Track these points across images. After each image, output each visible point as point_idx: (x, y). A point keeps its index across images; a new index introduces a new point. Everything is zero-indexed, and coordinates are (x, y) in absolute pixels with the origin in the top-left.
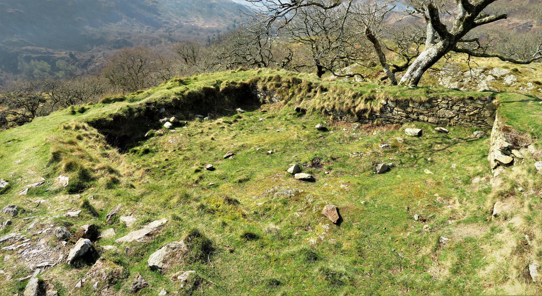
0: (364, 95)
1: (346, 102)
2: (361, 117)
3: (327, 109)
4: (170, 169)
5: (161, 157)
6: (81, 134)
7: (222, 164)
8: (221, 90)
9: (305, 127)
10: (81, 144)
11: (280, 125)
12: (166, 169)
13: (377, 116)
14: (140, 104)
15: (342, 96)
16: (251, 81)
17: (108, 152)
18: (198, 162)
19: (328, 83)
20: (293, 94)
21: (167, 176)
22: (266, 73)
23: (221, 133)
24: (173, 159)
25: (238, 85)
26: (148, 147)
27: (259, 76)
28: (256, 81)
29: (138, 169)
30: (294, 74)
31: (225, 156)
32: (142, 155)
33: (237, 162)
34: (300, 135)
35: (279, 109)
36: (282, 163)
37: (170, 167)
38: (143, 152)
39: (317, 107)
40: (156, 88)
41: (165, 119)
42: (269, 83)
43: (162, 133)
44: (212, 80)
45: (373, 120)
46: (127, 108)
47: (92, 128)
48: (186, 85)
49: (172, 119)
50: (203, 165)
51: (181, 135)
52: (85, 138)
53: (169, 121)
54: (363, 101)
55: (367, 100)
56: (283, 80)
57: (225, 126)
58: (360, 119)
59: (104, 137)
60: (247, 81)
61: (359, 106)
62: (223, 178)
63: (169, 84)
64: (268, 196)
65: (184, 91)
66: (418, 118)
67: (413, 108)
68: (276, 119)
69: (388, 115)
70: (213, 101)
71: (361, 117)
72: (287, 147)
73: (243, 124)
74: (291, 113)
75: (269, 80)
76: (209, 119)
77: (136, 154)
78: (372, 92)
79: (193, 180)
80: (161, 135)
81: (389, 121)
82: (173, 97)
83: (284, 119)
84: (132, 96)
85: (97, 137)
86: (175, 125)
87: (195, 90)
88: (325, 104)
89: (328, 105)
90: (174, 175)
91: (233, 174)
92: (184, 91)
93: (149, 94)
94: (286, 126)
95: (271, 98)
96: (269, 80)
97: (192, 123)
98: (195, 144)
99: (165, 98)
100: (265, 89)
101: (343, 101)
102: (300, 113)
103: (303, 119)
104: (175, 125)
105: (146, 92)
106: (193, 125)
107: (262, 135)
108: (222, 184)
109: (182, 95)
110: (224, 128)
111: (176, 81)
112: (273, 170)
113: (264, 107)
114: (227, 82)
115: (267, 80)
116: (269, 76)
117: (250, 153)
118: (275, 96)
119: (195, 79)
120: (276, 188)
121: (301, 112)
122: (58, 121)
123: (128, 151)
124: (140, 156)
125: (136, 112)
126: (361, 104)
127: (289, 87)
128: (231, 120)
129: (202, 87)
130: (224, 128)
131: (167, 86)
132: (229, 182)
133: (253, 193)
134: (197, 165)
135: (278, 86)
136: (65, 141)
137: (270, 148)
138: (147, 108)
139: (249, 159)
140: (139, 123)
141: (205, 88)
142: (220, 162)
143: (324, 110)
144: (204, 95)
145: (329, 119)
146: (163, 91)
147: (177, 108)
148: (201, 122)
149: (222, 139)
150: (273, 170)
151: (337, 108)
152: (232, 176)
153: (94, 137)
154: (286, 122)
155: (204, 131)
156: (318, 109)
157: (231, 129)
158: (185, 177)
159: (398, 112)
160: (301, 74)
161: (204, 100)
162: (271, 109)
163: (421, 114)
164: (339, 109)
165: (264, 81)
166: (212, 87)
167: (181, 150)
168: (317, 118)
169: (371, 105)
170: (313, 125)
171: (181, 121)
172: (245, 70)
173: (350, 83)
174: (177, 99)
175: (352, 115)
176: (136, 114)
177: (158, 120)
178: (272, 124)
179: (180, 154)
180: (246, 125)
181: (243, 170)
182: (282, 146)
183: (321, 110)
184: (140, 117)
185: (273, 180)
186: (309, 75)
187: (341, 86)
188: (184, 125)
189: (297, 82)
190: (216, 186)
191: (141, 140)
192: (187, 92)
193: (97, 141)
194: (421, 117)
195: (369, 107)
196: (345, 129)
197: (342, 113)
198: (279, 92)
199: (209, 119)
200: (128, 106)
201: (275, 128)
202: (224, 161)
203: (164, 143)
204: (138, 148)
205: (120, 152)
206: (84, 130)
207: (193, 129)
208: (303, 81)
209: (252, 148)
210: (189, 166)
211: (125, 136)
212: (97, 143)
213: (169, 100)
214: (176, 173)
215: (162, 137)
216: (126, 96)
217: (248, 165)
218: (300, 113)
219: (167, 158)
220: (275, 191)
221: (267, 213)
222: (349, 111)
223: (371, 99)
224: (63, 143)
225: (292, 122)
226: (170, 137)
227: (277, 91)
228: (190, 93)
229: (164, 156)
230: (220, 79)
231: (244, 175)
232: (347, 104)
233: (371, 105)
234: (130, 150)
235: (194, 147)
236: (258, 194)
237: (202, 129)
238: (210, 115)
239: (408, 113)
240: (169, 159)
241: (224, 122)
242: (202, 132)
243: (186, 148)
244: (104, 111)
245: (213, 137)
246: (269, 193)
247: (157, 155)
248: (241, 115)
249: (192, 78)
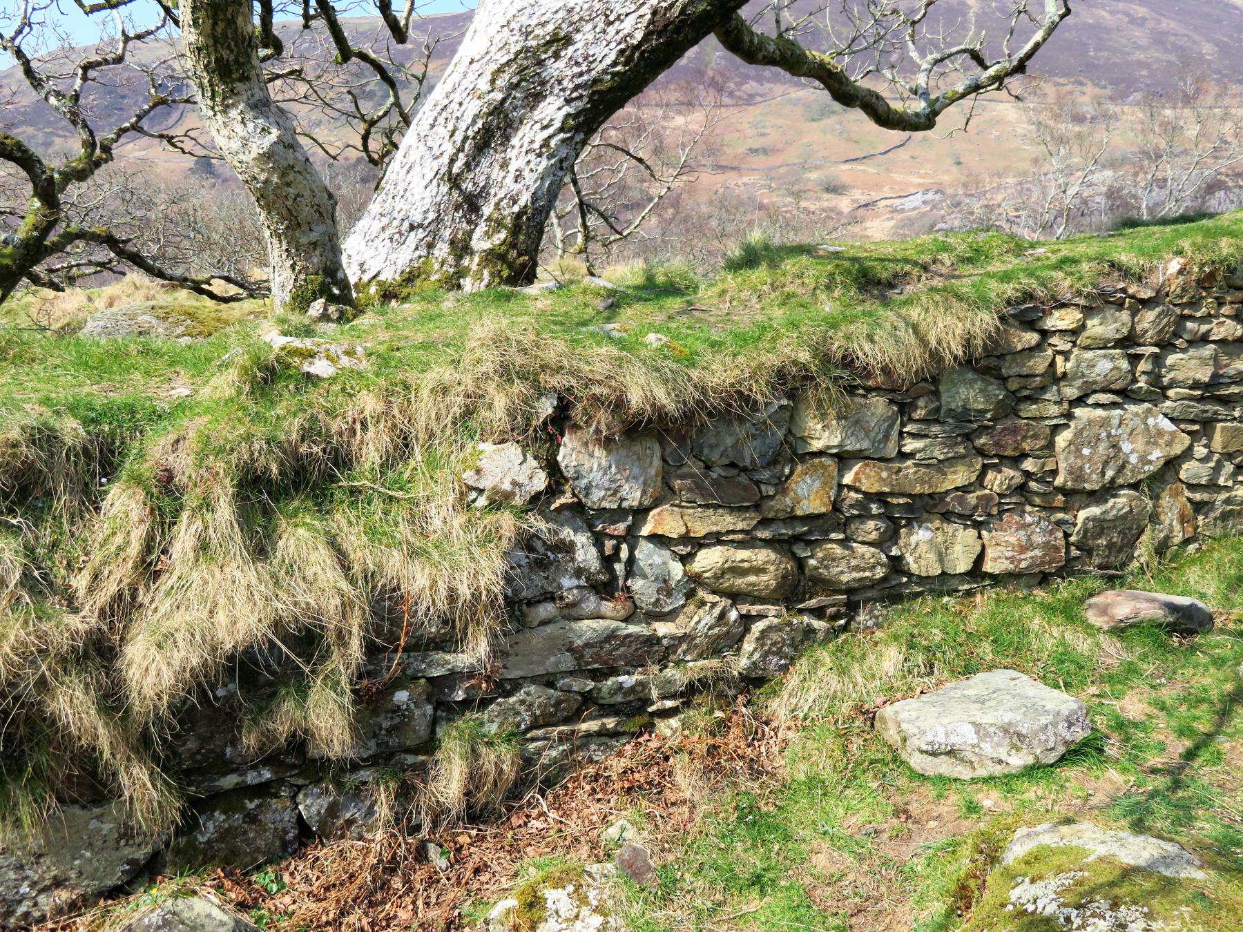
66: (896, 565)
67: (843, 459)
69: (588, 629)
81: (602, 700)
159: (691, 555)
163: (927, 507)
194: (921, 547)
239: (795, 536)
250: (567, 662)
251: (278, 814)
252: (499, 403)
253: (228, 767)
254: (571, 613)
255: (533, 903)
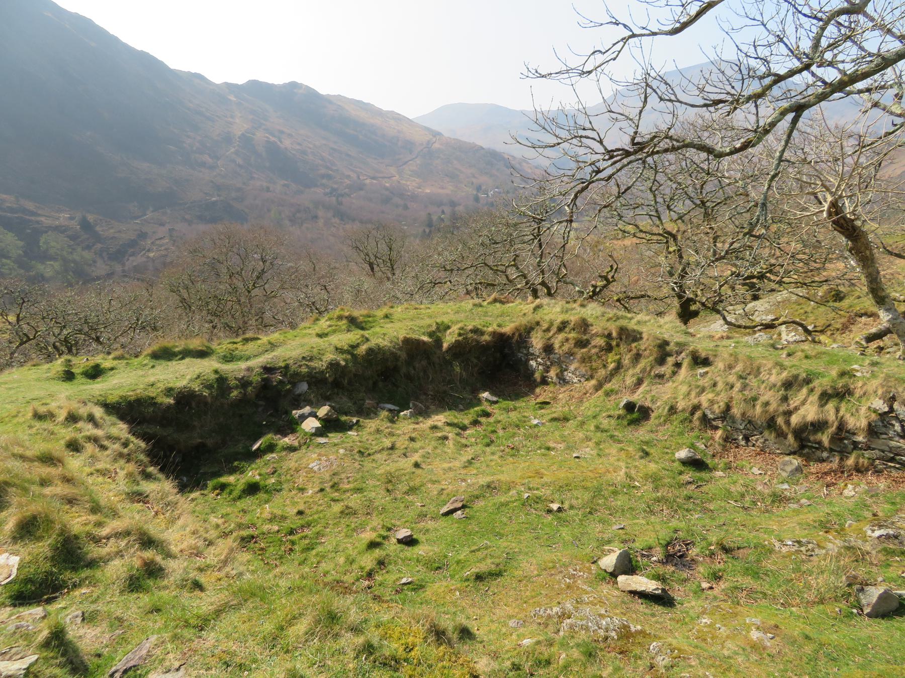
0: (816, 383)
1: (763, 399)
2: (805, 441)
3: (708, 412)
4: (305, 537)
5: (285, 505)
6: (79, 436)
7: (436, 529)
8: (445, 345)
9: (647, 454)
10: (75, 464)
11: (582, 441)
12: (296, 537)
13: (855, 445)
14: (249, 369)
15: (753, 382)
16: (517, 329)
17: (148, 487)
18: (376, 521)
19: (712, 344)
20: (619, 367)
21: (297, 556)
22: (553, 311)
23: (439, 451)
24: (317, 512)
25: (487, 338)
26: (258, 478)
27: (537, 317)
28: (529, 330)
29: (225, 535)
30: (623, 317)
31: (445, 509)
32: (240, 498)
33: (473, 526)
34: (633, 472)
35: (581, 401)
36: (585, 539)
37: (307, 532)
38: (244, 491)
39: (681, 405)
40: (292, 333)
41: (307, 410)
42: (561, 336)
43: (296, 444)
44: (428, 321)
45: (844, 454)
46: (213, 376)
47: (114, 419)
48: (363, 329)
49: (323, 411)
50: (389, 529)
51: (342, 451)
52: (90, 448)
53: (316, 417)
54: (814, 398)
55: (825, 397)
56: (594, 330)
57: (450, 435)
58: (802, 447)
59: (143, 445)
60: (507, 329)
61: (802, 411)
62: (437, 566)
63: (324, 324)
64: (546, 626)
65: (358, 345)
68: (572, 424)
70: (425, 372)
71: (805, 441)
72: (599, 499)
73: (494, 432)
74: (612, 413)
75: (561, 329)
76: (412, 415)
77: (225, 495)
78: (843, 374)
79: (362, 568)
80: (292, 449)
82: (329, 357)
83: (592, 428)
84: (231, 346)
85: (125, 445)
86: (330, 425)
87: (384, 343)
88: (704, 399)
89: (712, 402)
90: (314, 552)
91: (462, 557)
92: (358, 345)
93: (273, 346)
94: (598, 444)
95: (562, 371)
96: (561, 329)
97: (371, 425)
98: (374, 476)
99: (311, 359)
100: (548, 349)
101: (754, 393)
102: (635, 415)
103: (642, 433)
104: (330, 425)
105: (264, 339)
106: (372, 430)
107: (537, 461)
108: (433, 582)
109: (353, 355)
110: (446, 438)
111: (340, 318)
112: (561, 555)
113: (543, 393)
114: (462, 329)
115: (554, 329)
116: (559, 320)
117: (506, 504)
118: (572, 368)
119: (386, 316)
120: (569, 606)
121: (637, 414)
122: (20, 396)
123: (205, 487)
124: (234, 500)
125: (237, 387)
126: (807, 406)
127: (609, 348)
128: (465, 418)
129: (401, 337)
130: (446, 438)
131: (317, 329)
132: (452, 577)
133: (510, 611)
134: (374, 529)
135: (582, 344)
136: (29, 453)
137: (557, 496)
138: (263, 380)
139: (505, 519)
140: (241, 416)
141: (407, 341)
142: (430, 524)
143: (698, 414)
144: (403, 355)
145: (712, 438)
146: (306, 340)
147: (337, 384)
148: (392, 421)
149: (438, 466)
150: (561, 555)
151: (736, 411)
152: (458, 562)
153: (117, 446)
154: (599, 434)
155: (398, 445)
156: (683, 410)
157: (464, 441)
158: (342, 560)
160: (639, 317)
161: (404, 370)
162: (561, 400)
164: (743, 414)
165: (548, 330)
166: (425, 339)
167: (337, 490)
168: (681, 434)
169: (837, 410)
170: (668, 450)
171: (344, 418)
172: (502, 303)
173: (773, 346)
174: (338, 364)
175: (781, 435)
176: (234, 394)
177: (288, 413)
178: (562, 436)
179: (333, 500)
180: (501, 433)
181: (486, 548)
182: (587, 496)
183: (692, 413)
184: (243, 401)
185: (559, 582)
186: (662, 321)
187: (749, 352)
188: (350, 428)
189: (629, 336)
190: (418, 587)
191: (241, 460)
192: (363, 348)
193: (121, 455)
195: (831, 417)
196: (761, 469)
197: (751, 428)
198: (583, 360)
199: (412, 415)
200: (216, 372)
201: (569, 448)
202: (443, 523)
203: (297, 471)
204: (231, 479)
205: (183, 488)
206: (90, 426)
207: (371, 438)
208: (645, 336)
209: (513, 492)
210: (354, 530)
211: (201, 449)
212: (122, 462)
213: (320, 365)
214: (320, 549)
215: (294, 456)
216: (214, 346)
217: (500, 535)
218: (635, 415)
219: (301, 507)
220: (564, 615)
221: (541, 672)
222: (771, 424)
223: (840, 394)
224: (23, 458)
225: (612, 437)
226: (315, 456)
227: (579, 356)
228: (370, 351)
229: (294, 504)
230: (446, 319)
231: (489, 561)
232: (767, 404)
233: (837, 410)
234: (211, 484)
235: (371, 483)
236: (522, 615)
237: (394, 439)
238: (415, 406)
240: (307, 511)
241: (449, 424)
242: (392, 448)
243: (351, 486)
244: (152, 379)
245: (419, 460)
246: (550, 617)
247: (278, 499)
248: (489, 409)
249: (380, 313)
250: (887, 449)
251: (818, 453)
252: (880, 392)
253: (810, 441)
254: (891, 439)
255: (846, 485)
